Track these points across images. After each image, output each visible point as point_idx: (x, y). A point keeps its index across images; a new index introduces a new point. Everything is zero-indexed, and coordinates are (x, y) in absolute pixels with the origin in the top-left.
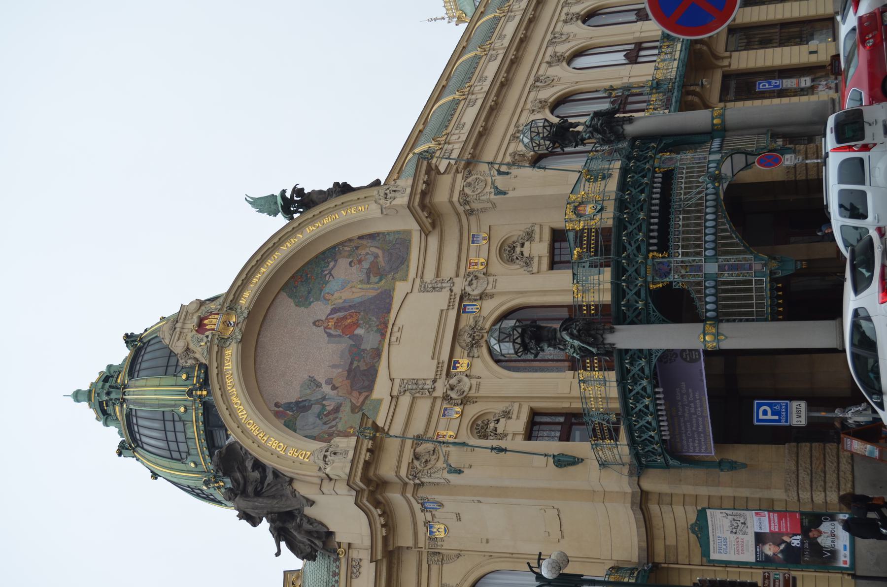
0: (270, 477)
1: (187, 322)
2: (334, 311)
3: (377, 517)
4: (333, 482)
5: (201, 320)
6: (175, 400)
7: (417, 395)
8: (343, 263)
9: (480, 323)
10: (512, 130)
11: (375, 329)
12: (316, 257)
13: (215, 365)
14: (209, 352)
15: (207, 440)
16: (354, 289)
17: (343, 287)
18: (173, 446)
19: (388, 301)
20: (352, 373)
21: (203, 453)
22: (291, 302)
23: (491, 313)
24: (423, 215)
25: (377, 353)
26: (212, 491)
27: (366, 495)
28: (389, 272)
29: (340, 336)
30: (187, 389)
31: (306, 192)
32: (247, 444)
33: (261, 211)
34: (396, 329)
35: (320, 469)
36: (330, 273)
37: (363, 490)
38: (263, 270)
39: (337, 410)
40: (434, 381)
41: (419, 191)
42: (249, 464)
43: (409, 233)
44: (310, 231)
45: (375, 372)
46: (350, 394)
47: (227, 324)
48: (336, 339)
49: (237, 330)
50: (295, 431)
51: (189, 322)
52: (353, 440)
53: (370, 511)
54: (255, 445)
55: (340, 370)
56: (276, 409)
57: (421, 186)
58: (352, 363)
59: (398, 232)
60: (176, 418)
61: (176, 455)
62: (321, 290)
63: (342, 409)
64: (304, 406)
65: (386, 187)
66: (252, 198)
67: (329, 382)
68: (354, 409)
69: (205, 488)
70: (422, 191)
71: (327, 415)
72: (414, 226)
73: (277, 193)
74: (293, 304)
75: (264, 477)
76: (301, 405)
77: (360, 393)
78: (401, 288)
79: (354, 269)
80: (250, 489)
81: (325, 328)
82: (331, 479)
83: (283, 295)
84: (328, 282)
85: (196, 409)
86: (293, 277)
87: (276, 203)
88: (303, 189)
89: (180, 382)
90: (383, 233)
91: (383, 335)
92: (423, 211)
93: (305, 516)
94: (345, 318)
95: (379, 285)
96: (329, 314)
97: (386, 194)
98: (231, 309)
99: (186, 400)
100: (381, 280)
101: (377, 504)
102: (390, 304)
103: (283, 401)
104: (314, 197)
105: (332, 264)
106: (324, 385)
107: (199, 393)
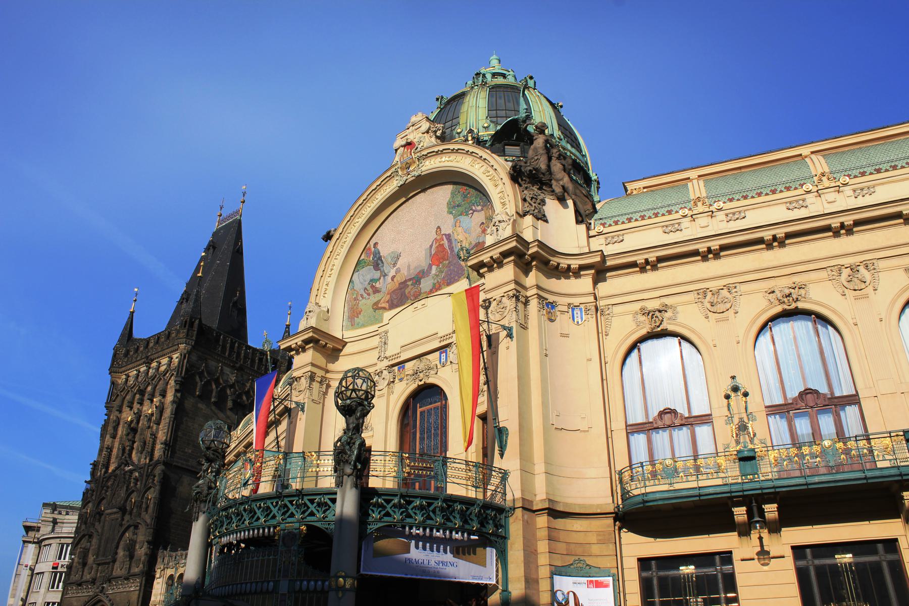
2: (448, 237)
9: (432, 372)
10: (713, 285)
20: (404, 284)
23: (440, 378)
25: (417, 297)
39: (376, 291)
40: (386, 358)
41: (481, 259)
58: (410, 280)
62: (461, 214)
64: (378, 265)
67: (398, 271)
71: (372, 287)
84: (467, 215)
91: (431, 291)
103: (379, 247)
105: (479, 208)
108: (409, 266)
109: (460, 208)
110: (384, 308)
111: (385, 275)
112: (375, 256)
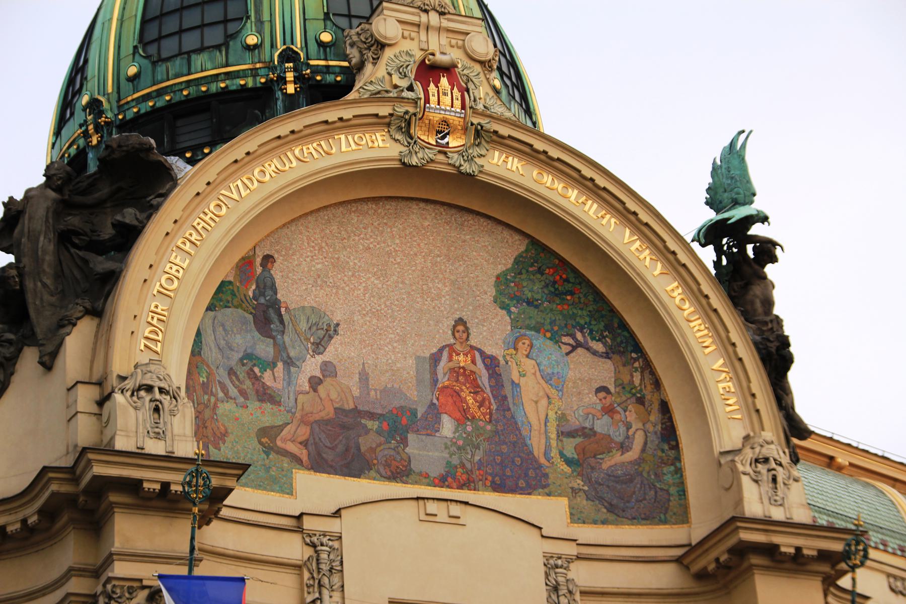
0: (101, 264)
1: (444, 36)
2: (491, 363)
3: (20, 516)
4: (95, 409)
5: (448, 69)
6: (272, 21)
7: (306, 575)
8: (604, 372)
11: (455, 461)
12: (613, 311)
13: (347, 114)
14: (377, 97)
15: (188, 100)
16: (544, 402)
17: (547, 378)
18: (171, 25)
19: (522, 483)
21: (160, 93)
22: (505, 262)
24: (720, 552)
25: (400, 472)
26: (80, 116)
27: (66, 488)
28: (588, 480)
29: (435, 381)
30: (298, 46)
31: (770, 270)
32: (173, 206)
33: (715, 170)
34: (455, 509)
35: (123, 378)
36: (579, 345)
37: (76, 480)
38: (573, 194)
39: (266, 396)
41: (776, 539)
42: (129, 215)
43: (683, 517)
44: (669, 292)
45: (356, 473)
46: (303, 421)
47: (443, 129)
48: (427, 376)
49: (429, 154)
50: (209, 308)
51: (444, 40)
52: (187, 448)
53: (36, 496)
54: (169, 226)
55: (356, 392)
56: (258, 260)
57: (787, 543)
58: (372, 416)
59: (683, 492)
60: (232, 28)
61: (153, 32)
63: (268, 406)
65: (785, 460)
66: (744, 146)
67: (328, 369)
68: (268, 436)
69: (85, 99)
70: (776, 547)
71: (251, 375)
72: (698, 530)
73: (759, 205)
74: (501, 268)
75: (100, 248)
76: (271, 311)
77: (305, 444)
78: (551, 510)
79: (592, 399)
80: (74, 221)
81: (450, 346)
82: (101, 403)
83: (519, 246)
84: (555, 339)
85: (254, 73)
86: (563, 262)
87: (736, 203)
88: (773, 259)
89: (312, 28)
90: (678, 458)
91: (442, 481)
92: (731, 551)
93: (20, 351)
94: (476, 389)
95: (557, 460)
96: (482, 353)
97: (766, 460)
98: (478, 134)
99: (273, 46)
100: (569, 462)
101: (49, 513)
102: (514, 490)
103: (277, 272)
104: (757, 290)
105: (599, 347)
106: (319, 359)
107: (290, 76)
108: (364, 377)
109: (533, 312)
110: (298, 460)
111: (289, 363)
112: (261, 291)
